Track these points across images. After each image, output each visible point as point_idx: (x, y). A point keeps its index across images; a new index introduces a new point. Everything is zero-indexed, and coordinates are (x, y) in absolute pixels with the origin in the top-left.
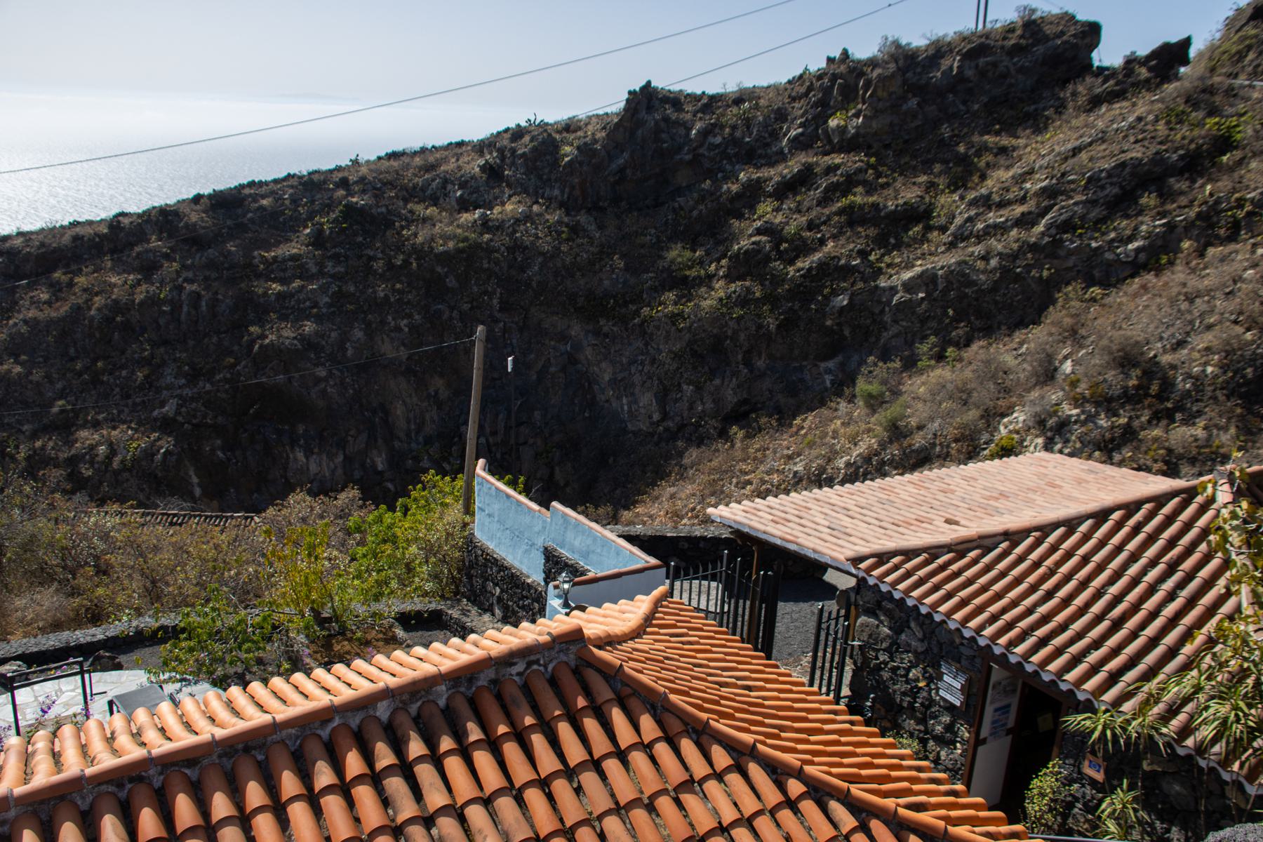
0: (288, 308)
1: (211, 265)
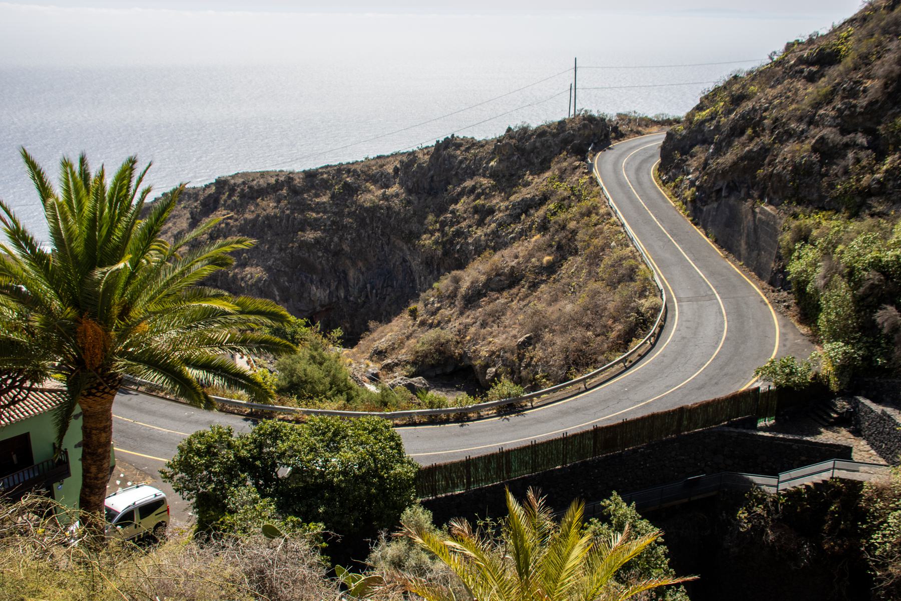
0: (314, 225)
1: (298, 203)
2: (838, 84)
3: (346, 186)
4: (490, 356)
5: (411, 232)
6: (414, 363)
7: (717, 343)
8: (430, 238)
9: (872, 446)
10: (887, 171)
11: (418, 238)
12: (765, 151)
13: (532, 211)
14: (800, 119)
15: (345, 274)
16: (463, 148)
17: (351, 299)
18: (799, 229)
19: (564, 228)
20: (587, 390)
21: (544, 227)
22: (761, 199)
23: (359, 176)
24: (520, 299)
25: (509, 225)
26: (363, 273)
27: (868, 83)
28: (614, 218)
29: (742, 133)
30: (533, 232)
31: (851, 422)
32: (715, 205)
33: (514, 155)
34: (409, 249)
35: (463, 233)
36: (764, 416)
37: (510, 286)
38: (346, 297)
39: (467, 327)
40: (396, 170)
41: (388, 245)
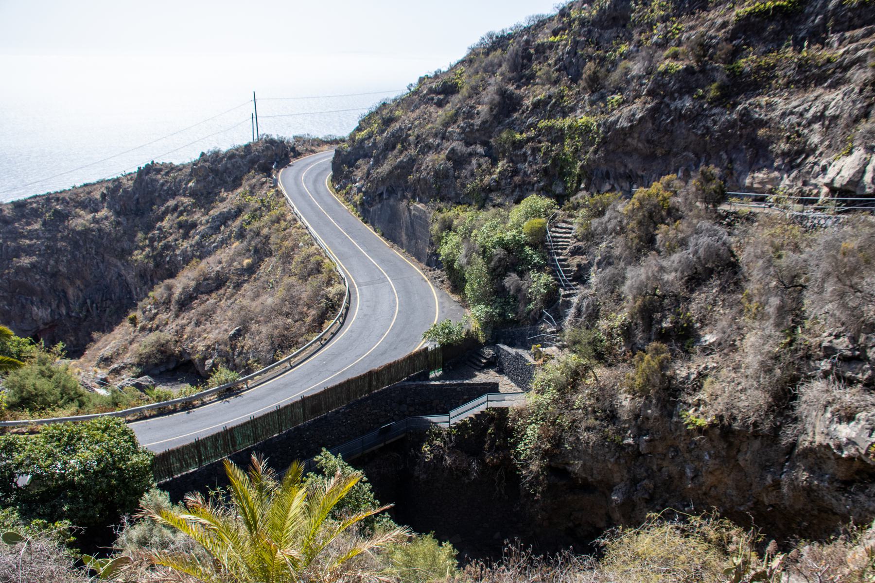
0: (29, 251)
1: (10, 232)
2: (459, 108)
3: (57, 213)
4: (207, 350)
5: (123, 250)
6: (139, 365)
7: (392, 316)
8: (141, 254)
9: (512, 379)
10: (500, 173)
11: (131, 254)
12: (412, 161)
13: (230, 223)
14: (436, 136)
15: (65, 292)
16: (163, 173)
17: (73, 314)
18: (444, 221)
19: (258, 234)
20: (292, 368)
21: (241, 235)
22: (414, 198)
23: (68, 203)
24: (227, 298)
25: (211, 236)
26: (81, 290)
27: (480, 108)
28: (300, 223)
29: (394, 148)
30: (232, 240)
31: (495, 364)
32: (379, 206)
33: (209, 176)
34: (123, 265)
35: (171, 246)
36: (433, 369)
37: (218, 288)
38: (68, 314)
39: (183, 327)
40: (103, 196)
41: (103, 262)
